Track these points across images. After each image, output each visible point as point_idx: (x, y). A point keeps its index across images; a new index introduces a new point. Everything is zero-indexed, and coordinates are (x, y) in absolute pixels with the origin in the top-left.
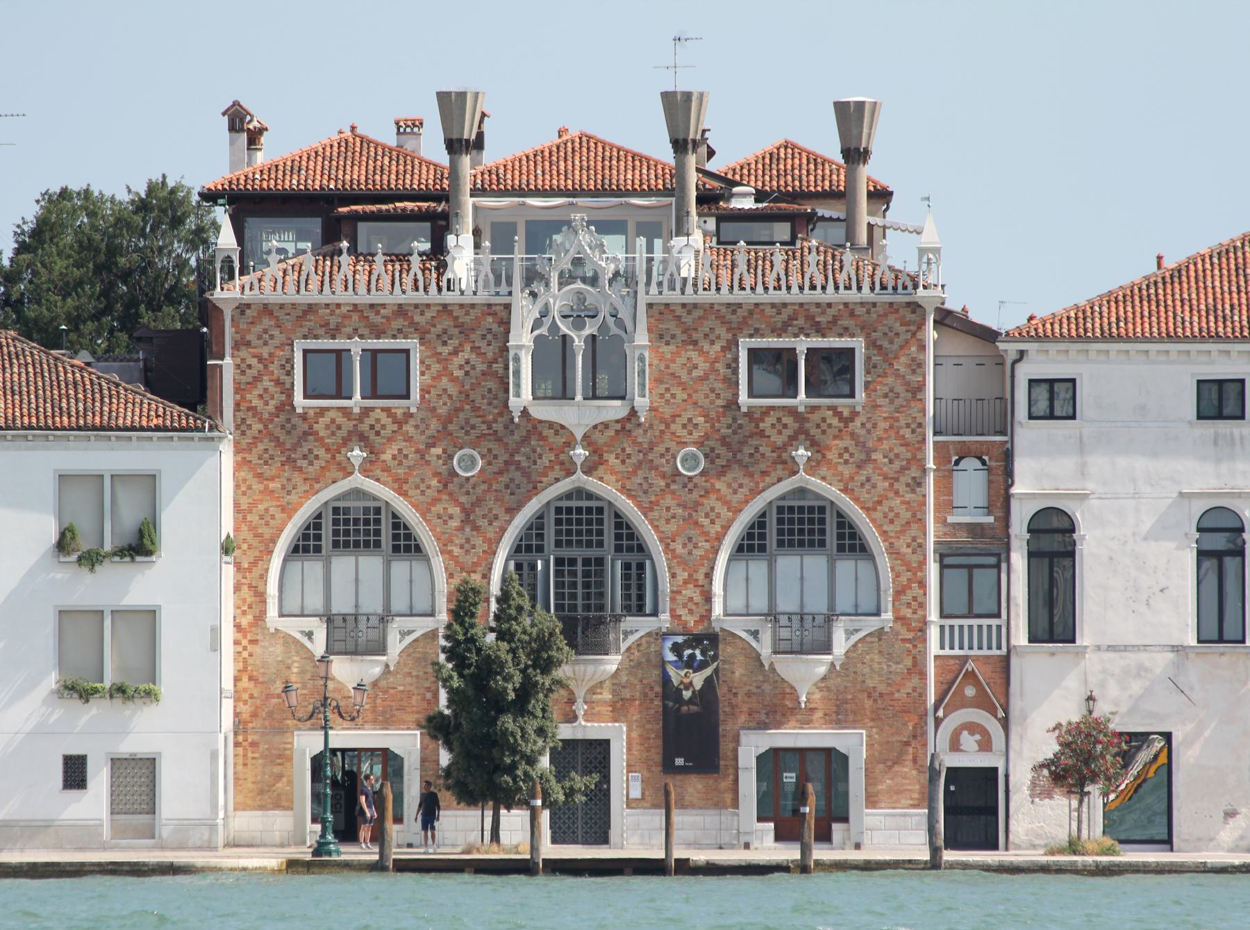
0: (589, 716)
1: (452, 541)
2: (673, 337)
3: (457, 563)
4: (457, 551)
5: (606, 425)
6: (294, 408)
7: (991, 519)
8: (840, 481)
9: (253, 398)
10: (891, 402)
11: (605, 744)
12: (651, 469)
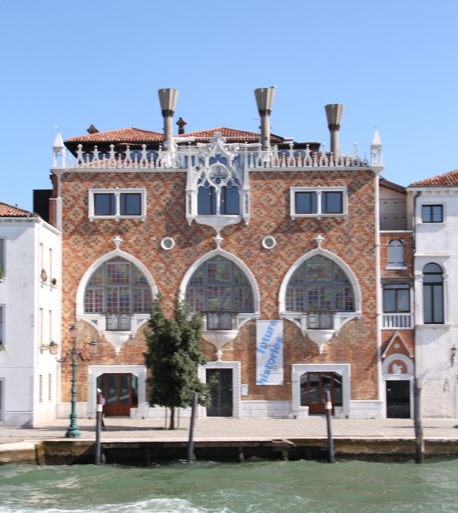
0: (224, 358)
2: (261, 186)
3: (164, 289)
4: (163, 283)
5: (230, 226)
6: (88, 219)
7: (405, 268)
8: (337, 251)
9: (70, 215)
10: (360, 215)
11: (230, 371)
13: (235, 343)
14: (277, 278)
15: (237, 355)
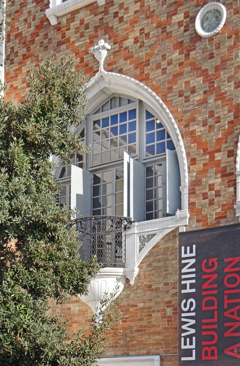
1: (193, 120)
3: (200, 145)
4: (199, 129)
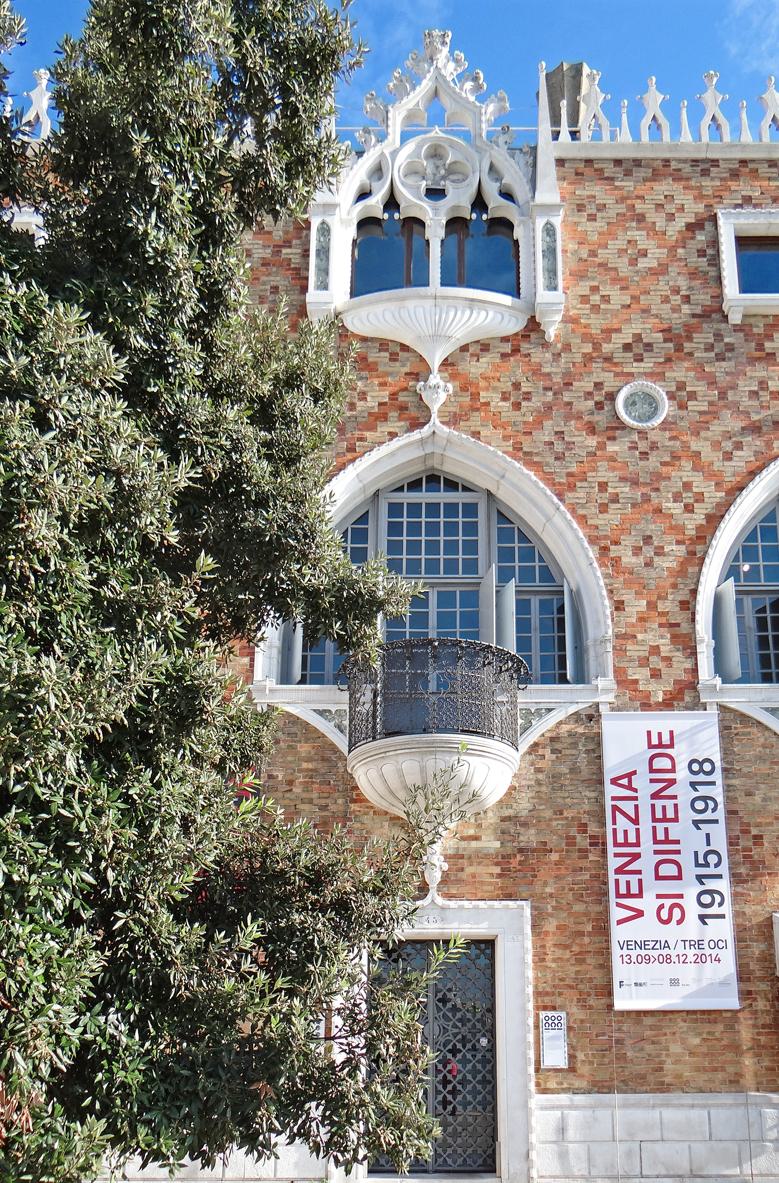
2: (602, 208)
12: (568, 418)
13: (504, 819)
14: (678, 543)
15: (514, 871)
